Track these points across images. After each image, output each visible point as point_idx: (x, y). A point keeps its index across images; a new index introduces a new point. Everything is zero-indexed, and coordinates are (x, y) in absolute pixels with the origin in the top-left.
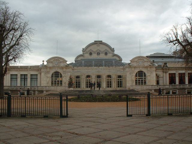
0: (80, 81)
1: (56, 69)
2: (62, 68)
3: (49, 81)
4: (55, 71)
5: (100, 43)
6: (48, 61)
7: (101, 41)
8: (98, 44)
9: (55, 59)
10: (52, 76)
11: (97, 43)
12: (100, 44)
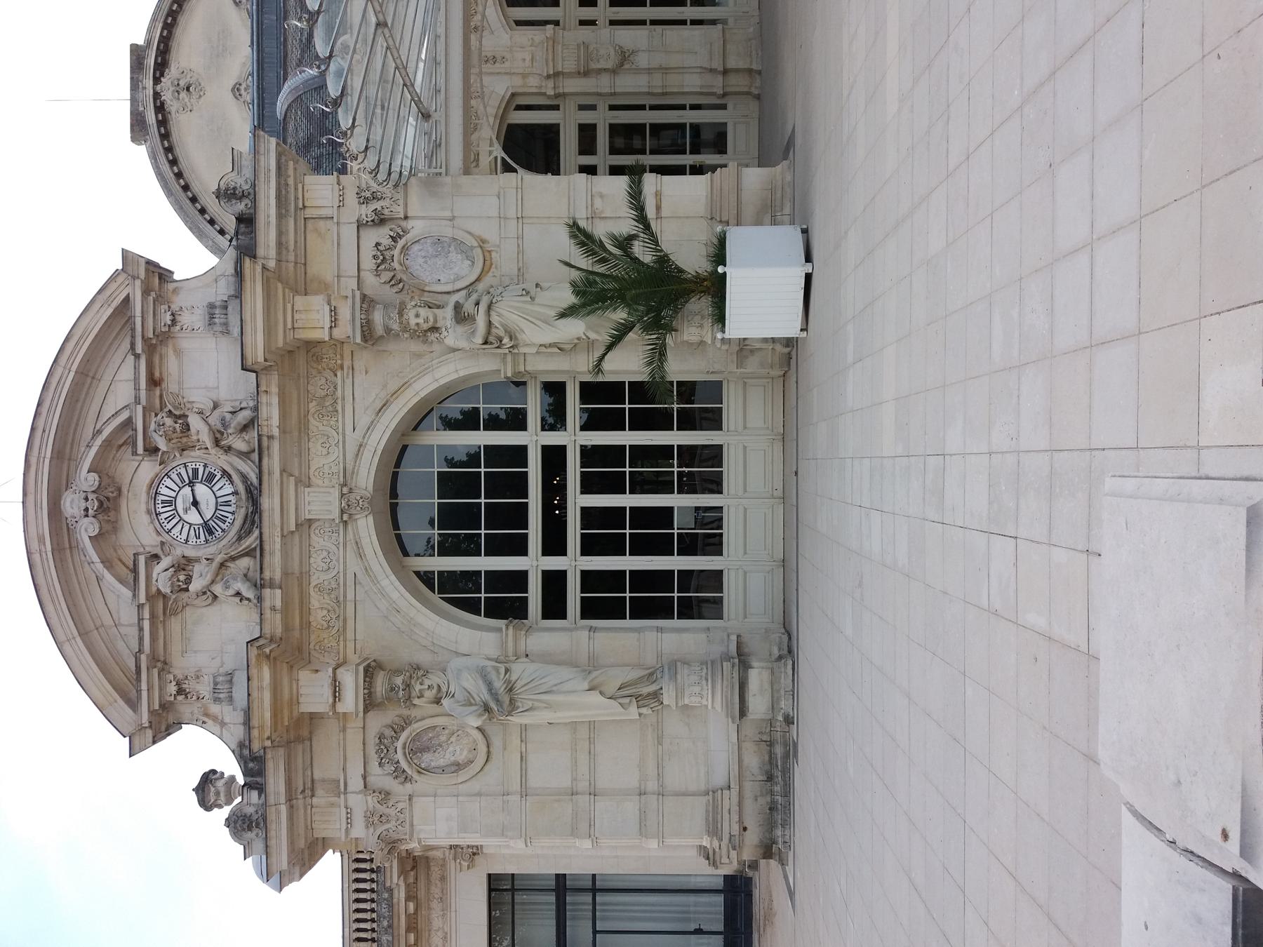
0: (602, 119)
1: (322, 502)
2: (297, 364)
3: (590, 666)
4: (366, 527)
5: (154, 60)
6: (146, 703)
7: (137, 54)
8: (167, 96)
9: (87, 529)
10: (497, 610)
11: (160, 108)
12: (172, 72)
